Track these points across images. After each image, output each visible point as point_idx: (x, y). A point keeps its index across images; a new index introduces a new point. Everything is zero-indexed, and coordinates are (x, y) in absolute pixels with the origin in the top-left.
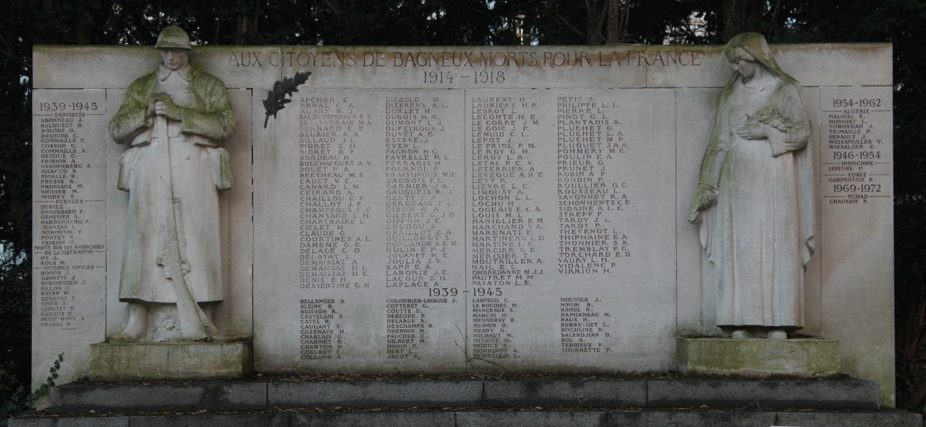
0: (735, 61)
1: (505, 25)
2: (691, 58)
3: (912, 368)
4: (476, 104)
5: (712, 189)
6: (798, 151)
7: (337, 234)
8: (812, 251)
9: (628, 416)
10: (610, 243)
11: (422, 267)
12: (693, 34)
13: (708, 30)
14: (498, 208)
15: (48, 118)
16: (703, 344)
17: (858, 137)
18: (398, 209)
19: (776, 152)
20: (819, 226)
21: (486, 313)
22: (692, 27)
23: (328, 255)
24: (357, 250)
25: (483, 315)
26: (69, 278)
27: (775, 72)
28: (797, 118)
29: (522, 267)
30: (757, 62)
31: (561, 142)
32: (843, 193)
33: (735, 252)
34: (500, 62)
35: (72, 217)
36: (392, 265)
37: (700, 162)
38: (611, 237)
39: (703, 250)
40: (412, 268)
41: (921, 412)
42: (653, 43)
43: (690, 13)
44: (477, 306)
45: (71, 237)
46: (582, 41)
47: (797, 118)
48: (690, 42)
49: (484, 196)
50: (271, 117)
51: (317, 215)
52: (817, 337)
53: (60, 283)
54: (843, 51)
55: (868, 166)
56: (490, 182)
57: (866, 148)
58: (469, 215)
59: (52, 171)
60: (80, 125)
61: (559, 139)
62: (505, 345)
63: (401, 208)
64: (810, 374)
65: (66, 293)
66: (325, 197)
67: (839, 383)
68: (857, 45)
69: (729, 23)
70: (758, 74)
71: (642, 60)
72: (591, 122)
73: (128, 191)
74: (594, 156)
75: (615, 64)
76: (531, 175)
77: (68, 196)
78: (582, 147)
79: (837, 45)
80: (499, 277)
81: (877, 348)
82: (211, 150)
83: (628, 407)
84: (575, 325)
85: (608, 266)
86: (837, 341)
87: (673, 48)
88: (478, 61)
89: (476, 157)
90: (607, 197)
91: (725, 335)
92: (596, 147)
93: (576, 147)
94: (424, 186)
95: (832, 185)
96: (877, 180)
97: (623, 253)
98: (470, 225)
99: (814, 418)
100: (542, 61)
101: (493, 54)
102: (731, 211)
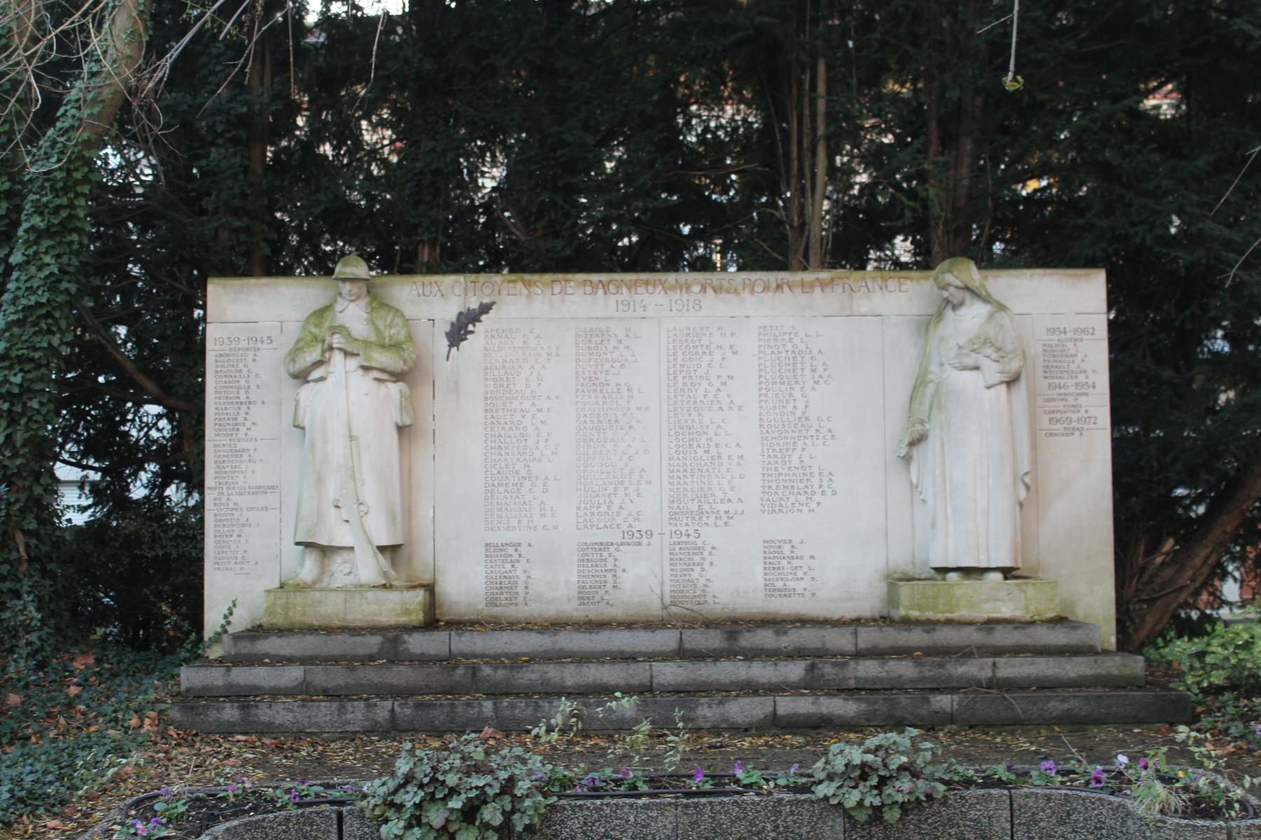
0: (944, 287)
1: (701, 251)
2: (897, 284)
3: (1131, 608)
4: (671, 334)
5: (922, 422)
6: (1011, 382)
7: (523, 473)
8: (1028, 488)
9: (834, 665)
11: (615, 508)
12: (898, 258)
13: (915, 254)
14: (695, 444)
15: (223, 353)
16: (915, 587)
17: (1073, 367)
18: (589, 447)
19: (989, 383)
20: (1034, 461)
21: (683, 557)
22: (897, 252)
23: (514, 495)
24: (545, 491)
25: (681, 559)
26: (243, 520)
27: (986, 299)
28: (1010, 347)
29: (722, 508)
30: (967, 288)
31: (762, 373)
32: (1059, 426)
33: (948, 489)
34: (696, 289)
35: (245, 455)
36: (583, 506)
37: (909, 393)
38: (816, 474)
39: (914, 487)
40: (604, 508)
41: (1141, 654)
42: (856, 269)
43: (894, 237)
44: (674, 549)
45: (245, 477)
46: (783, 267)
47: (1010, 347)
48: (895, 268)
49: (681, 431)
50: (454, 350)
51: (503, 452)
52: (1035, 578)
53: (233, 525)
54: (1055, 277)
55: (1084, 398)
56: (687, 417)
57: (1081, 378)
59: (226, 409)
60: (254, 360)
61: (760, 370)
62: (704, 591)
63: (592, 444)
64: (1028, 617)
65: (239, 536)
66: (511, 433)
67: (1059, 626)
68: (1070, 271)
69: (936, 248)
70: (968, 301)
71: (847, 286)
72: (793, 352)
73: (303, 428)
74: (797, 388)
75: (818, 290)
76: (730, 408)
77: (241, 435)
78: (786, 380)
79: (1049, 271)
80: (697, 517)
81: (1096, 588)
82: (390, 385)
83: (835, 656)
84: (779, 568)
85: (813, 505)
86: (1056, 582)
87: (879, 274)
88: (673, 288)
89: (672, 390)
90: (812, 432)
91: (939, 577)
92: (800, 379)
93: (778, 379)
94: (617, 421)
95: (1047, 417)
96: (1093, 412)
97: (829, 491)
98: (665, 462)
99: (1033, 664)
100: (741, 288)
101: (689, 281)
102: (943, 445)
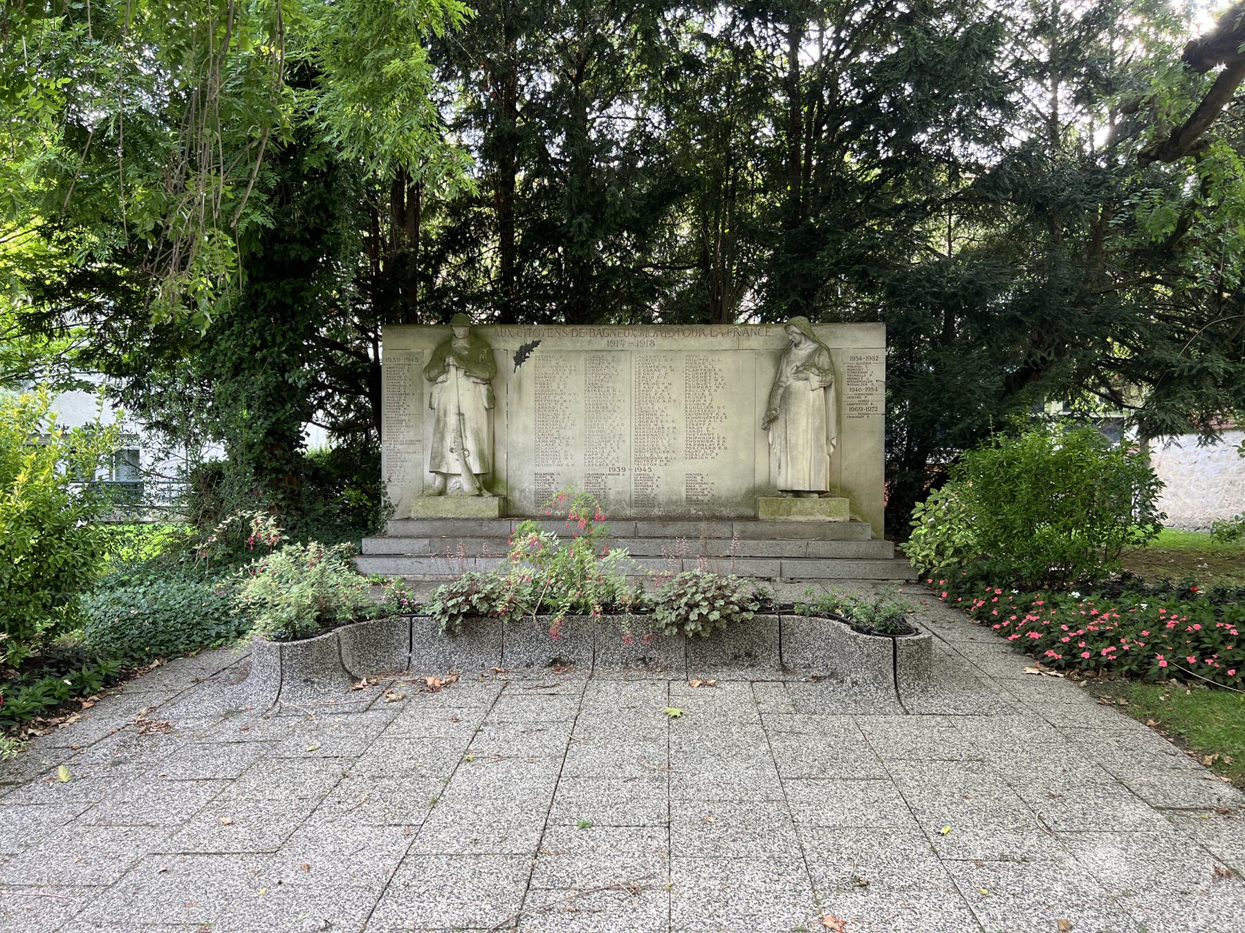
10: (715, 442)
11: (605, 455)
17: (864, 379)
35: (404, 424)
40: (599, 455)
58: (633, 424)
70: (803, 341)
82: (482, 386)
85: (714, 455)
90: (714, 415)
98: (633, 430)
